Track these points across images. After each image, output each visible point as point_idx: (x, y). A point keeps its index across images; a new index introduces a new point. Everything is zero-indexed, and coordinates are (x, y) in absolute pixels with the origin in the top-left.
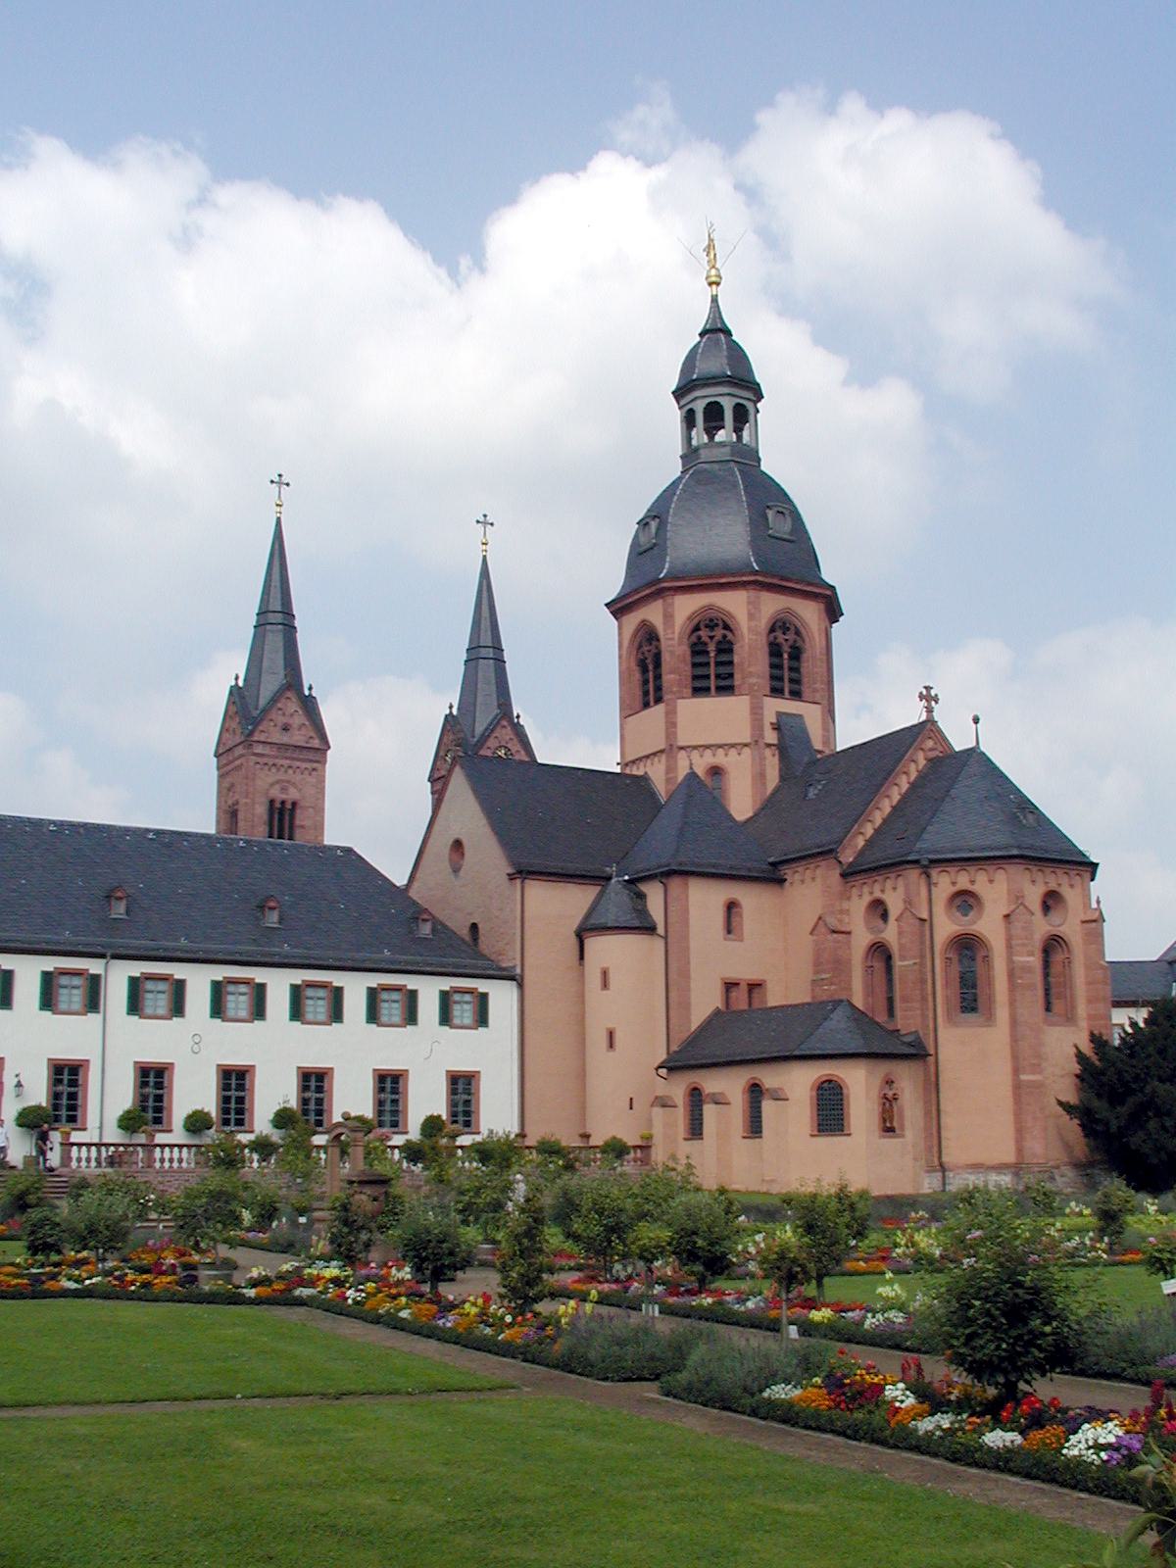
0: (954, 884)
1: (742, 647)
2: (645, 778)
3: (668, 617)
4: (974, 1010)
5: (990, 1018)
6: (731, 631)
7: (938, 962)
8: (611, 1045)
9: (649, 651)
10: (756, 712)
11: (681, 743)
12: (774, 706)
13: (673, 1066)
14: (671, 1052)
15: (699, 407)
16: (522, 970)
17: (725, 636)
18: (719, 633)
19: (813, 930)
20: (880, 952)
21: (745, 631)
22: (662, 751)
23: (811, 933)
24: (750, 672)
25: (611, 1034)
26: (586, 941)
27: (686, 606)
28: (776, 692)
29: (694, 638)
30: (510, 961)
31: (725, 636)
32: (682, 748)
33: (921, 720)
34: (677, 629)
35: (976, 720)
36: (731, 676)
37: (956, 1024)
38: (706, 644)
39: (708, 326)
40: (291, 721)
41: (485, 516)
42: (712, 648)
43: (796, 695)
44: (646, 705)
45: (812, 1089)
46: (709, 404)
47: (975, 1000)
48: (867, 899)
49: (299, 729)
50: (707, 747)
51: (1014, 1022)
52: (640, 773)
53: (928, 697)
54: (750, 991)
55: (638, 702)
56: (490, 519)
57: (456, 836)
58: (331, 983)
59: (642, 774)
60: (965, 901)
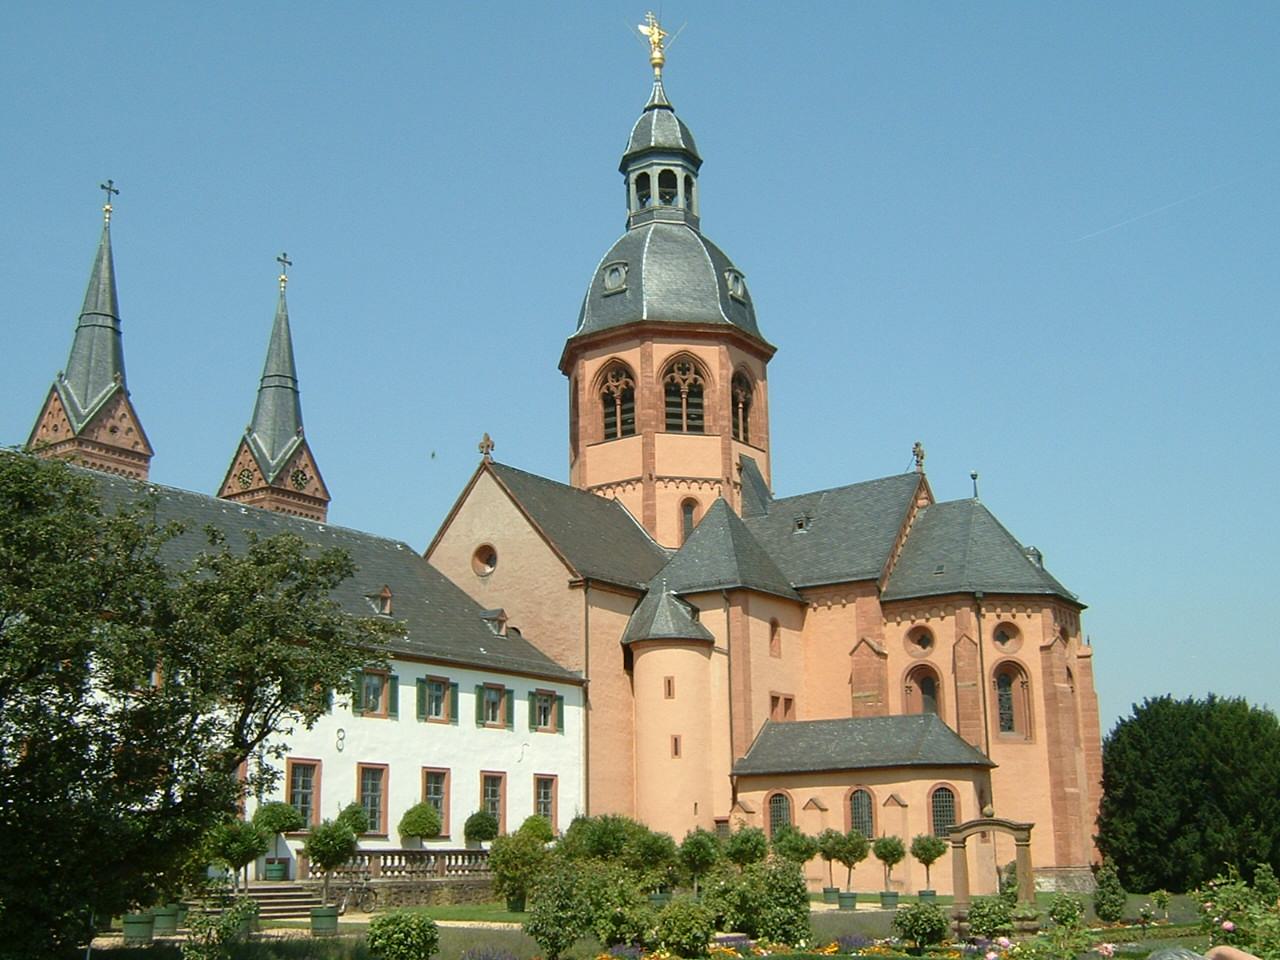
0: (999, 616)
1: (714, 391)
2: (614, 503)
3: (647, 358)
4: (1010, 728)
5: (1030, 737)
6: (702, 376)
7: (987, 684)
8: (676, 752)
9: (617, 387)
10: (726, 451)
11: (659, 472)
12: (738, 448)
13: (742, 778)
14: (736, 760)
15: (654, 173)
16: (587, 676)
17: (696, 380)
18: (691, 377)
19: (856, 648)
20: (925, 679)
21: (717, 378)
22: (639, 480)
23: (851, 654)
24: (722, 416)
26: (635, 653)
27: (663, 351)
28: (736, 436)
29: (668, 379)
30: (573, 663)
31: (696, 380)
32: (660, 479)
33: (909, 472)
34: (655, 370)
35: (974, 477)
36: (700, 417)
37: (1003, 741)
38: (678, 386)
39: (656, 102)
40: (118, 424)
41: (285, 255)
42: (685, 388)
43: (746, 441)
44: (610, 436)
45: (928, 797)
46: (664, 171)
47: (1012, 720)
48: (907, 625)
49: (127, 434)
50: (683, 480)
51: (1054, 741)
52: (609, 495)
53: (919, 454)
54: (786, 703)
55: (601, 435)
56: (288, 259)
58: (448, 679)
59: (612, 498)
60: (1005, 633)
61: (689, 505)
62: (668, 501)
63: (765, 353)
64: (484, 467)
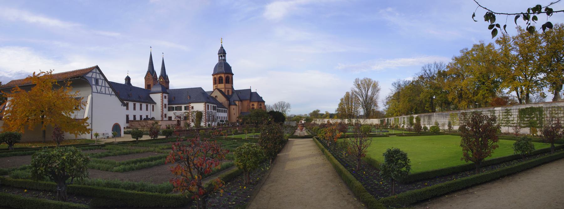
25: (234, 114)
32: (226, 88)
44: (220, 83)
57: (216, 95)
61: (228, 91)
62: (227, 90)
63: (233, 74)
64: (216, 88)
